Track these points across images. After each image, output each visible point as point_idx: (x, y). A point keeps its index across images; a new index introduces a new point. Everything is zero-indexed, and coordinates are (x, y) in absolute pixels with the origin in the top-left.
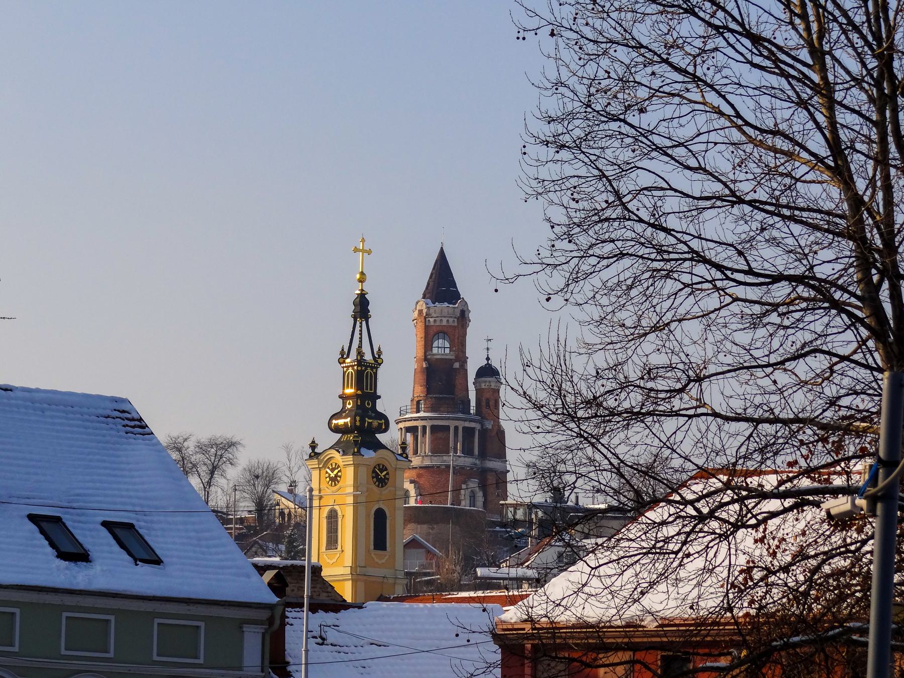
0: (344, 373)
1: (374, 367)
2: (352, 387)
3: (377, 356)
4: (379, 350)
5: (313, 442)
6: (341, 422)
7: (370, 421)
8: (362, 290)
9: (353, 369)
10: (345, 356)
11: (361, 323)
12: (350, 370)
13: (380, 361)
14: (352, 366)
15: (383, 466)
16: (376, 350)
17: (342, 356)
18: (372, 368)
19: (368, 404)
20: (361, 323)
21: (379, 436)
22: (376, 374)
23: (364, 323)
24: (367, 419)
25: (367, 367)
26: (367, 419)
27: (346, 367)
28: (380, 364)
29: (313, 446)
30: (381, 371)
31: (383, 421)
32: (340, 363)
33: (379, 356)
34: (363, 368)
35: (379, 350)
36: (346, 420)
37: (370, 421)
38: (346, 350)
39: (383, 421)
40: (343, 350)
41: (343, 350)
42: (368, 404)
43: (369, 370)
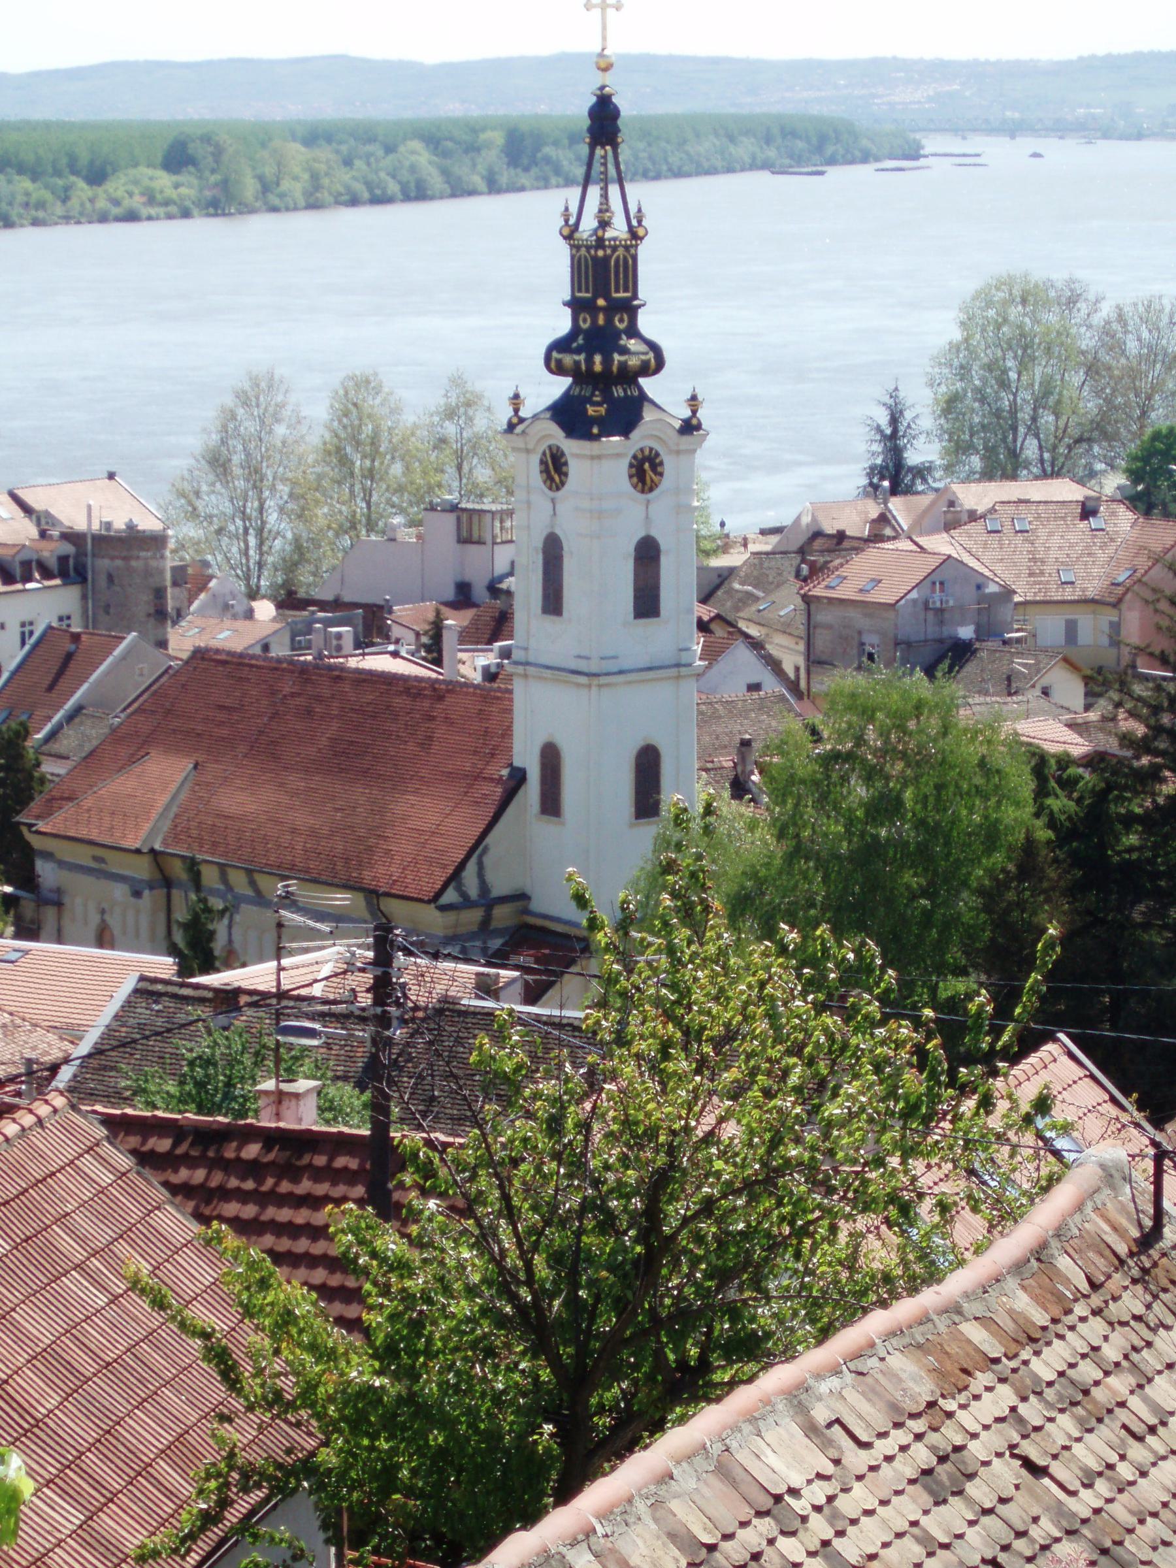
0: (573, 257)
2: (587, 291)
3: (634, 223)
4: (639, 210)
5: (516, 396)
6: (568, 360)
7: (623, 358)
8: (602, 88)
13: (641, 232)
15: (651, 449)
16: (633, 210)
17: (567, 221)
18: (627, 248)
19: (621, 321)
20: (605, 157)
21: (642, 381)
22: (635, 258)
25: (614, 249)
26: (617, 357)
28: (641, 239)
30: (644, 252)
32: (565, 238)
33: (640, 222)
34: (609, 251)
35: (639, 210)
36: (577, 358)
37: (623, 358)
38: (574, 209)
40: (567, 209)
41: (567, 209)
43: (620, 252)
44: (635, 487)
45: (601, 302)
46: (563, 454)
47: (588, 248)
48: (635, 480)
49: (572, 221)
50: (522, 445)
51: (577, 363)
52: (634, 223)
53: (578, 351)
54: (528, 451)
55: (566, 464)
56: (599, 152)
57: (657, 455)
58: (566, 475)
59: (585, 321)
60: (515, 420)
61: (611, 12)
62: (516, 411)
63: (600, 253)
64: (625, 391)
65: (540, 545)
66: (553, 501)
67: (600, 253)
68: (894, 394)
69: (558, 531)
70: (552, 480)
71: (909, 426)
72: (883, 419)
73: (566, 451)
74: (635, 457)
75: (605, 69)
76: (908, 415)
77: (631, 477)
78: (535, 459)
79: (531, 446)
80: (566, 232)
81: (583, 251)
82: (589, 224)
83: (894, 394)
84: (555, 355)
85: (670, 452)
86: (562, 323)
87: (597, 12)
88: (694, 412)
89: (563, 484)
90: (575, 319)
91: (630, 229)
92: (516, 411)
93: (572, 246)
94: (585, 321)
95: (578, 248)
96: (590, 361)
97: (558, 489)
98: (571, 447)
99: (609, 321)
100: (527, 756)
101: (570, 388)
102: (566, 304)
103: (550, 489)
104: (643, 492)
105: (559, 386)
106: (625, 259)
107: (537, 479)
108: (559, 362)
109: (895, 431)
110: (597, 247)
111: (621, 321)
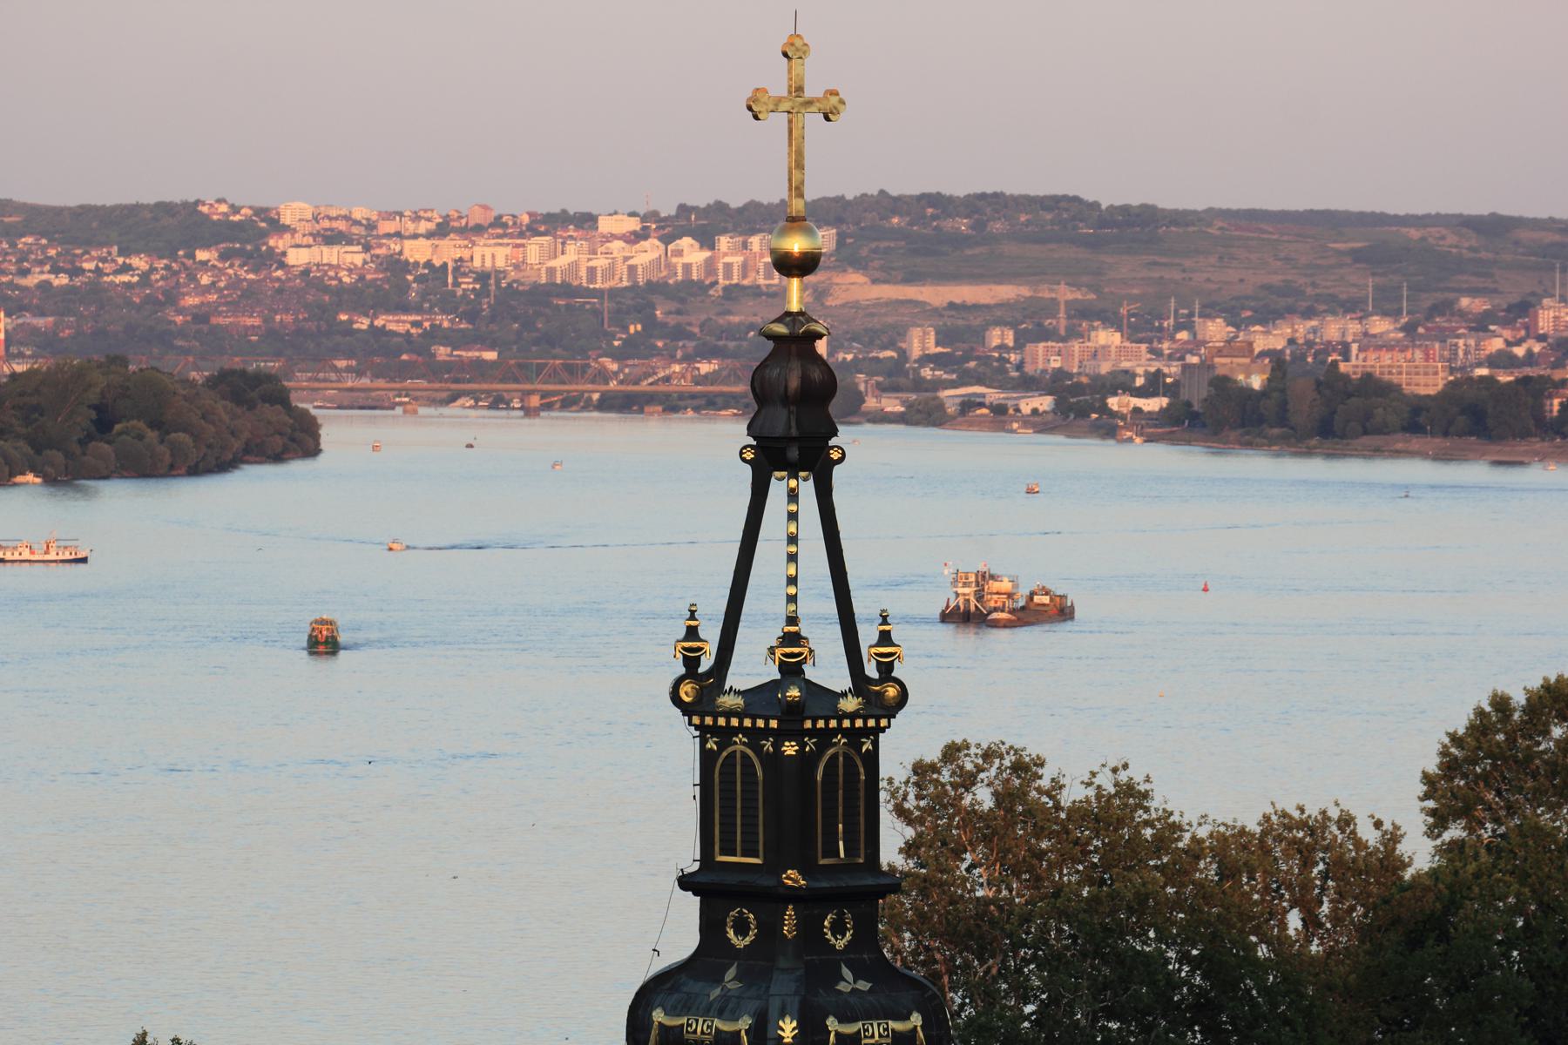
0: (707, 759)
1: (866, 732)
3: (871, 671)
4: (885, 638)
10: (706, 663)
11: (793, 496)
12: (739, 743)
13: (892, 692)
16: (867, 635)
17: (691, 663)
18: (855, 736)
20: (793, 496)
22: (872, 760)
23: (807, 489)
24: (832, 1023)
25: (825, 736)
26: (832, 1023)
27: (714, 730)
31: (916, 1019)
32: (687, 710)
33: (886, 669)
34: (810, 745)
35: (885, 638)
37: (849, 1029)
38: (711, 634)
39: (916, 1019)
40: (692, 633)
41: (692, 633)
42: (838, 929)
45: (793, 877)
47: (754, 735)
49: (706, 663)
52: (871, 671)
53: (725, 1009)
56: (778, 488)
59: (742, 929)
61: (813, 120)
63: (790, 749)
67: (790, 749)
80: (687, 692)
81: (739, 743)
84: (658, 1016)
87: (777, 123)
90: (710, 926)
91: (860, 681)
95: (726, 734)
99: (810, 931)
102: (686, 882)
106: (849, 761)
110: (780, 736)
111: (838, 929)
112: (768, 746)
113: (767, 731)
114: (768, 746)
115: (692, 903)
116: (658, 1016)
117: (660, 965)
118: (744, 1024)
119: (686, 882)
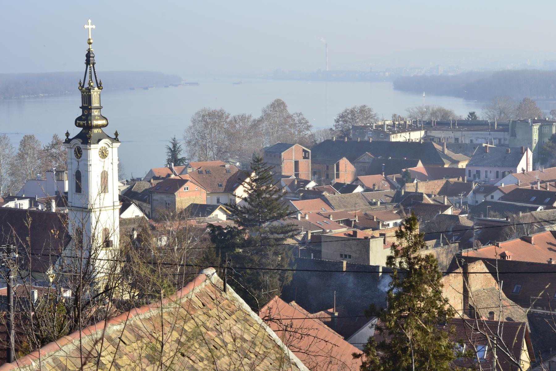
0: (82, 95)
3: (99, 85)
4: (100, 82)
6: (81, 123)
8: (89, 49)
9: (86, 93)
10: (82, 85)
13: (101, 88)
14: (86, 92)
15: (105, 147)
16: (99, 82)
17: (80, 85)
29: (67, 134)
33: (100, 85)
35: (100, 82)
38: (82, 82)
40: (80, 81)
41: (80, 81)
44: (101, 157)
46: (81, 149)
47: (86, 92)
48: (101, 155)
49: (82, 85)
50: (69, 147)
51: (84, 124)
52: (99, 85)
54: (71, 148)
55: (81, 151)
56: (89, 67)
57: (107, 148)
58: (82, 154)
59: (86, 112)
60: (67, 140)
62: (67, 137)
63: (90, 94)
64: (97, 131)
65: (75, 174)
66: (78, 162)
68: (174, 139)
69: (80, 170)
70: (78, 156)
71: (178, 148)
72: (171, 146)
73: (81, 148)
74: (100, 149)
75: (90, 43)
76: (178, 145)
77: (99, 154)
78: (73, 150)
79: (72, 147)
81: (85, 93)
82: (86, 85)
83: (174, 139)
84: (78, 121)
85: (109, 147)
86: (80, 113)
88: (117, 137)
89: (81, 157)
92: (67, 137)
93: (82, 92)
94: (86, 112)
95: (84, 92)
96: (87, 123)
97: (79, 158)
98: (82, 146)
100: (71, 232)
101: (82, 130)
102: (80, 108)
103: (77, 158)
104: (103, 158)
105: (79, 130)
107: (74, 156)
108: (79, 123)
109: (174, 150)
111: (96, 112)
112: (88, 93)
113: (87, 92)
114: (88, 93)
115: (81, 110)
116: (78, 121)
117: (78, 116)
118: (85, 122)
119: (80, 108)
